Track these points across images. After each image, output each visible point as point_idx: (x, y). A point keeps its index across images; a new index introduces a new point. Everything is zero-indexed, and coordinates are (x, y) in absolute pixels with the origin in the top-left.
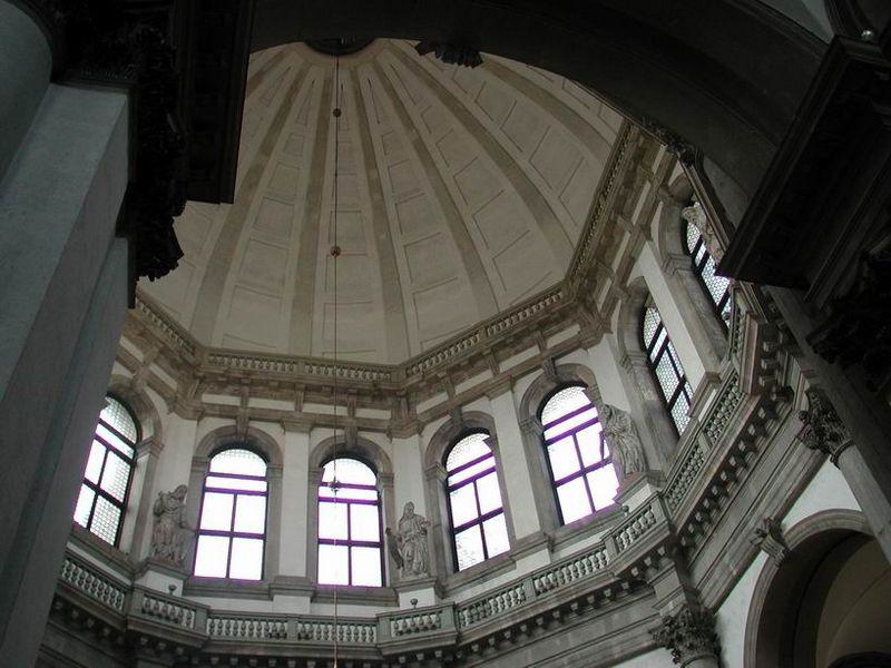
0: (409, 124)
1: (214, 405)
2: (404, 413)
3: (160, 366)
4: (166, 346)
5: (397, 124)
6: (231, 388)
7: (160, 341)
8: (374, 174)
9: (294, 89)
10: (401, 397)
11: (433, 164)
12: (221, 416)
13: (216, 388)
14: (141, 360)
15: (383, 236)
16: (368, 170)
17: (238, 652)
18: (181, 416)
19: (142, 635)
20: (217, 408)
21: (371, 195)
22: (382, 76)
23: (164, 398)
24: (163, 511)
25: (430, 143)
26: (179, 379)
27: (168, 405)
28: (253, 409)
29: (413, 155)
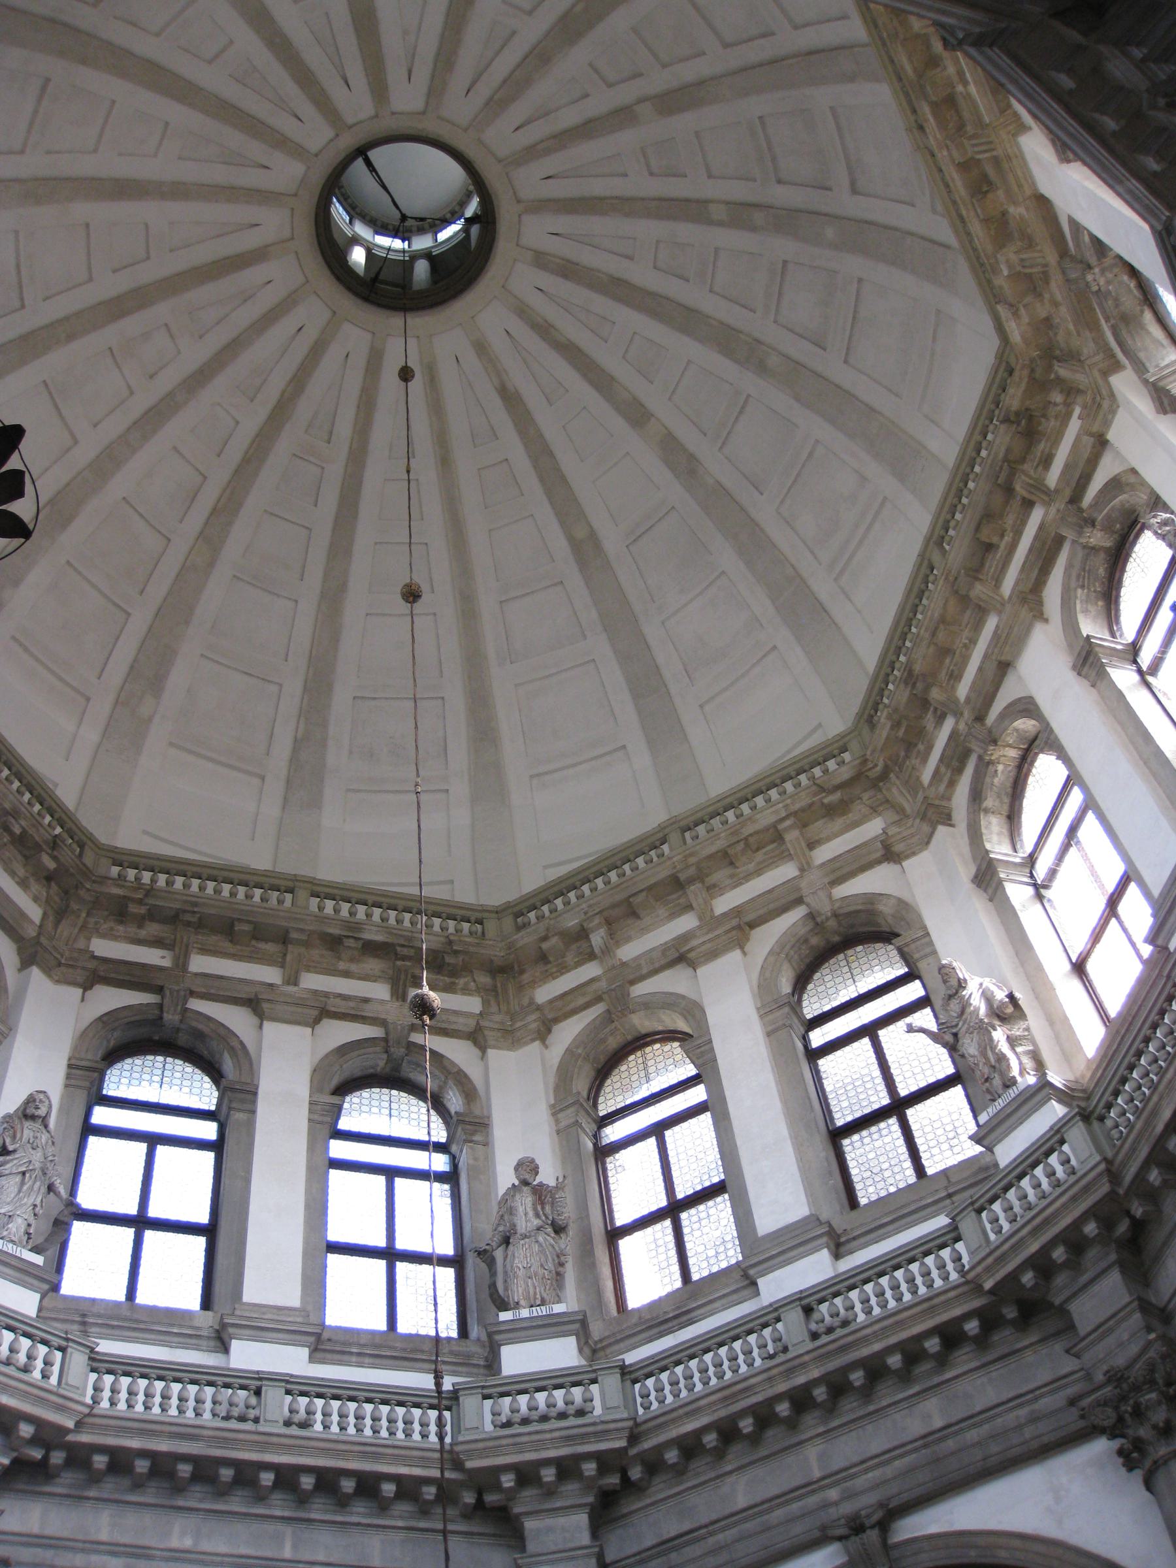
0: (623, 116)
1: (936, 773)
2: (1080, 378)
3: (829, 839)
4: (795, 814)
5: (626, 139)
6: (929, 720)
7: (783, 820)
8: (718, 212)
9: (544, 330)
10: (1049, 368)
11: (700, 83)
12: (960, 770)
13: (921, 747)
14: (797, 873)
15: (830, 233)
16: (710, 222)
17: (1160, 1127)
18: (921, 851)
19: (1014, 1276)
20: (943, 769)
21: (753, 229)
22: (532, 153)
23: (879, 862)
24: (955, 1035)
25: (659, 81)
26: (875, 811)
27: (895, 862)
28: (968, 700)
29: (684, 123)
